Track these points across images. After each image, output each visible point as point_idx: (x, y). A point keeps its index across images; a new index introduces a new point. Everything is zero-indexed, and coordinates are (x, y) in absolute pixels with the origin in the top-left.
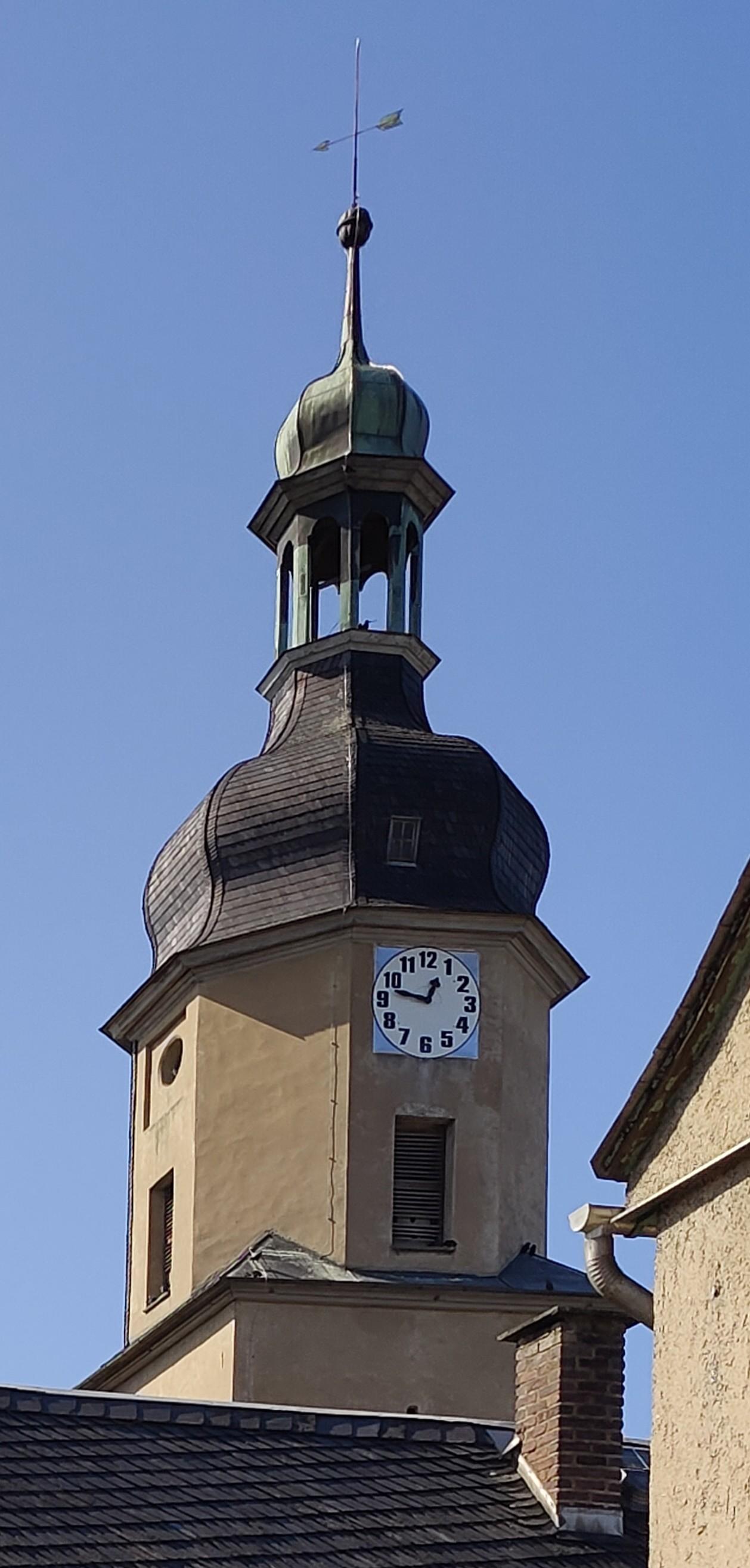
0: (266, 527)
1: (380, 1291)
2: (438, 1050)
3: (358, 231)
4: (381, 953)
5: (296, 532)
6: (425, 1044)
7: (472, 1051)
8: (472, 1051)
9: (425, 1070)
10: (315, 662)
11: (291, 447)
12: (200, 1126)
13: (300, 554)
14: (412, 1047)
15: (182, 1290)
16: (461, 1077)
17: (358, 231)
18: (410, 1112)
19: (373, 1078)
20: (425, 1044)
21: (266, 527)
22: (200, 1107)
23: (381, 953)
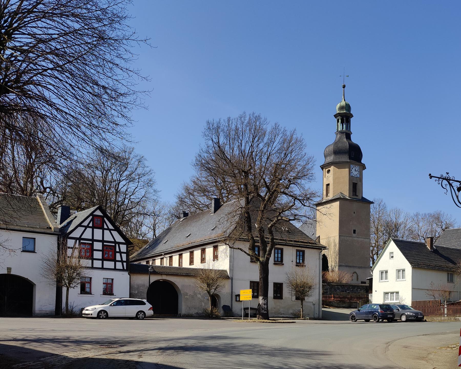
0: (336, 116)
1: (351, 200)
3: (344, 87)
4: (351, 165)
7: (359, 176)
8: (359, 176)
10: (341, 132)
12: (333, 180)
13: (340, 121)
14: (354, 175)
15: (331, 197)
16: (358, 179)
17: (344, 87)
21: (336, 116)
22: (333, 178)
23: (351, 165)
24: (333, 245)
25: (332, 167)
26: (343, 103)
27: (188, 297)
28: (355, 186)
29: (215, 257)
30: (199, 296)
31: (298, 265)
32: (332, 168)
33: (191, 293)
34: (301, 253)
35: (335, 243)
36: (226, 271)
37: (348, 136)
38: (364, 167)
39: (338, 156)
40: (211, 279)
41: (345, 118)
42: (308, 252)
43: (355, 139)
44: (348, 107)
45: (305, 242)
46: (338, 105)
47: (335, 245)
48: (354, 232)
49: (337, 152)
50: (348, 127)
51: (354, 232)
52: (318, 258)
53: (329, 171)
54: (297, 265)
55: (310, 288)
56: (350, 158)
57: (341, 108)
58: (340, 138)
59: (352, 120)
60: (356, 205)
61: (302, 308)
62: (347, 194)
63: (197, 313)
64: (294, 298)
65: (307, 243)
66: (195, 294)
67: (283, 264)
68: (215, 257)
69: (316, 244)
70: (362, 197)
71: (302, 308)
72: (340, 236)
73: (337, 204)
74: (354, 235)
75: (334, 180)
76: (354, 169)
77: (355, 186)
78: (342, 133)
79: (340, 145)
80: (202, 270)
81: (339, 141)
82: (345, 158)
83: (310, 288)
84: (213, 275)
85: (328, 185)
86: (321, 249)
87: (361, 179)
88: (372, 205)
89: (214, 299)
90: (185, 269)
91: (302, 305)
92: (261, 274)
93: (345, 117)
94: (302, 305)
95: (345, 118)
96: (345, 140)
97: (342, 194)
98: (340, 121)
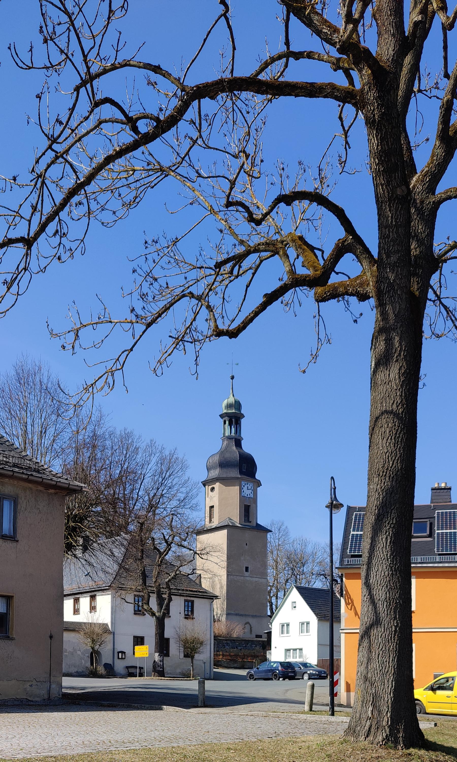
2: (249, 496)
3: (233, 378)
5: (227, 418)
6: (247, 495)
9: (247, 499)
10: (229, 438)
11: (225, 407)
12: (219, 501)
13: (227, 422)
14: (246, 495)
15: (216, 523)
16: (251, 500)
17: (233, 378)
18: (246, 504)
19: (242, 498)
20: (247, 495)
24: (218, 586)
25: (218, 484)
26: (231, 400)
27: (67, 654)
28: (248, 509)
29: (93, 608)
30: (79, 653)
31: (187, 617)
32: (217, 485)
33: (71, 649)
34: (190, 604)
35: (221, 583)
36: (107, 625)
37: (238, 443)
38: (259, 484)
39: (225, 470)
40: (95, 634)
41: (233, 420)
42: (198, 602)
43: (247, 447)
44: (237, 405)
45: (194, 591)
46: (225, 402)
47: (221, 587)
48: (247, 569)
49: (224, 464)
50: (238, 431)
51: (247, 569)
52: (209, 609)
53: (213, 489)
54: (185, 618)
55: (202, 643)
56: (241, 473)
57: (229, 406)
58: (228, 446)
59: (243, 421)
60: (248, 535)
61: (192, 666)
62: (237, 520)
63: (77, 672)
64: (182, 655)
65: (196, 591)
66: (75, 650)
67: (170, 617)
68: (93, 608)
69: (206, 593)
70: (257, 524)
71: (192, 666)
72: (228, 575)
73: (225, 532)
74: (247, 574)
75: (221, 501)
76: (246, 486)
77: (248, 509)
78: (230, 439)
79: (227, 455)
80: (85, 623)
81: (226, 448)
82: (235, 473)
83: (202, 643)
84: (96, 630)
85: (212, 507)
86: (212, 599)
87: (255, 500)
88: (269, 535)
89: (95, 655)
90: (68, 623)
91: (192, 663)
92: (157, 630)
93: (234, 418)
94: (192, 663)
95: (233, 420)
96: (234, 448)
97: (230, 519)
98: (227, 422)
